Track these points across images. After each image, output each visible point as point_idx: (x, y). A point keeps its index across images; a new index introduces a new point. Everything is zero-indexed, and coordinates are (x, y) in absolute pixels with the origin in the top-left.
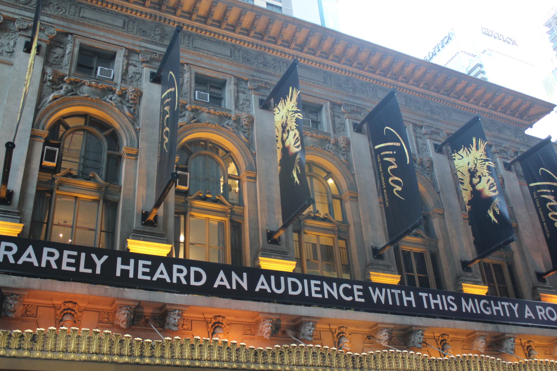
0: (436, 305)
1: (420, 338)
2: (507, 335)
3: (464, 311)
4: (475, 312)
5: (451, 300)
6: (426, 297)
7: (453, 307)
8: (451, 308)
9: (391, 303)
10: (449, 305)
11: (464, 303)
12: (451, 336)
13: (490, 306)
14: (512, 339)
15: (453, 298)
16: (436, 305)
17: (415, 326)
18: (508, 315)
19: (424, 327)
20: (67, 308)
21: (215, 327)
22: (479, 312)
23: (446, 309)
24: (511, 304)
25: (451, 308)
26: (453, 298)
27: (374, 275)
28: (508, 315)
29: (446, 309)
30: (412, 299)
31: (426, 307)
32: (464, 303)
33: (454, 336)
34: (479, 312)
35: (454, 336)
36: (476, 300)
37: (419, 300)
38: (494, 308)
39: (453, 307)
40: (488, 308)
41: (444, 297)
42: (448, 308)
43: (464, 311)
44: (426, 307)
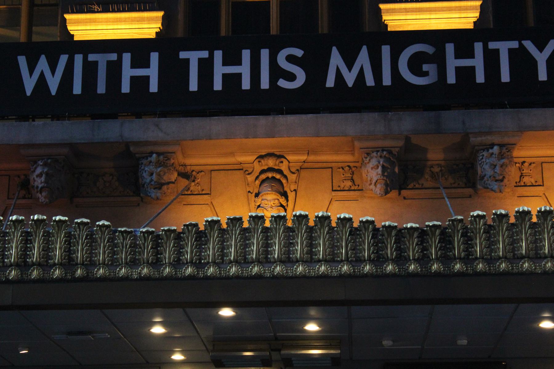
0: (232, 80)
1: (152, 174)
2: (474, 140)
3: (330, 82)
4: (370, 81)
5: (291, 59)
6: (200, 61)
7: (291, 77)
8: (282, 83)
9: (77, 89)
10: (277, 72)
11: (336, 60)
12: (291, 158)
13: (439, 60)
14: (496, 149)
15: (299, 53)
16: (232, 80)
17: (138, 144)
18: (505, 77)
19: (166, 143)
20: (266, 168)
21: (263, 182)
22: (387, 81)
23: (265, 84)
24: (529, 45)
25: (282, 83)
26: (299, 53)
27: (78, 22)
28: (505, 77)
29: (265, 84)
30: (152, 72)
31: (193, 86)
32: (336, 60)
33: (304, 158)
34: (387, 81)
35: (304, 158)
36: (386, 50)
37: (173, 71)
38: (453, 63)
39: (291, 77)
40: (425, 67)
41: (265, 54)
42: (273, 80)
43: (330, 82)
44: (193, 86)
